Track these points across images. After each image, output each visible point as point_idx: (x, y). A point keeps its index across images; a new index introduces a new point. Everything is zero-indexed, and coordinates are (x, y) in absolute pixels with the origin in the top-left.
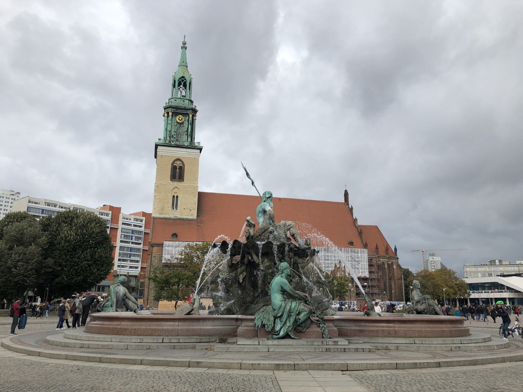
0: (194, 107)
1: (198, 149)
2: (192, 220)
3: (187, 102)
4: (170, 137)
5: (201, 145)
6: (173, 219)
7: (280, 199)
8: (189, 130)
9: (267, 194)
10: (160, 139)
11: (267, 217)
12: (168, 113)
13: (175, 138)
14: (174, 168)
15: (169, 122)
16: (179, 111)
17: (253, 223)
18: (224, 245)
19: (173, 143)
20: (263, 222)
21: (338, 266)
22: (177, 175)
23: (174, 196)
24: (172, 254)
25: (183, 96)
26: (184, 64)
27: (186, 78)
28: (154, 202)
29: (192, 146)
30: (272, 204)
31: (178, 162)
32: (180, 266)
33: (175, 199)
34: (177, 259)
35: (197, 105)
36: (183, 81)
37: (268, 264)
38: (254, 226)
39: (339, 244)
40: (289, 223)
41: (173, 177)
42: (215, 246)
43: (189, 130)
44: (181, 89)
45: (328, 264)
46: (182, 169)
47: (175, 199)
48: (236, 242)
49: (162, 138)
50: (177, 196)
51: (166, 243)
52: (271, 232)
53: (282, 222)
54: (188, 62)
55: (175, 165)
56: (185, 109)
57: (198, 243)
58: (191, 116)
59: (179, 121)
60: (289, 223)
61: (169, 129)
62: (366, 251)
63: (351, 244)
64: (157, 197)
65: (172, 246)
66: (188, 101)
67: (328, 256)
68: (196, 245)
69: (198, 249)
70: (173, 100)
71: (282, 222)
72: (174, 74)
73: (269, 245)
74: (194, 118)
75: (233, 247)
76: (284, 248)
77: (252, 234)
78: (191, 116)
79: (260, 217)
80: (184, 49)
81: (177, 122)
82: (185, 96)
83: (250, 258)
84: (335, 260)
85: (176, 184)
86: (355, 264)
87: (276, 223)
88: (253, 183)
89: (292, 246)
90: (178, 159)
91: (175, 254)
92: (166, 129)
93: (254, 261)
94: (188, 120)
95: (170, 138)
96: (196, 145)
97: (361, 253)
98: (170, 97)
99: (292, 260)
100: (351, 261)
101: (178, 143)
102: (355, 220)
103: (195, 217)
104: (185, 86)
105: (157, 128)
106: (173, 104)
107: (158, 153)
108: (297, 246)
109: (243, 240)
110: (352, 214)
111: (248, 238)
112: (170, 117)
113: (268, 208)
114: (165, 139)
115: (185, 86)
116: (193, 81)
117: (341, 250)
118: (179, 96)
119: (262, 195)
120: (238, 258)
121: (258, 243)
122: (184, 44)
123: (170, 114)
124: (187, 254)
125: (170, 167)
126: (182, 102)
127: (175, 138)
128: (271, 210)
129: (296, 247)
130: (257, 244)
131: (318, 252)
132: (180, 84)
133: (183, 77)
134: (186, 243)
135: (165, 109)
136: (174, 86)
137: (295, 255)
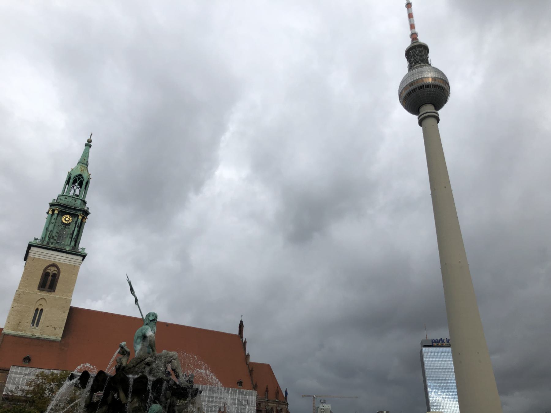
0: (86, 208)
3: (79, 202)
4: (49, 238)
5: (86, 252)
6: (30, 338)
7: (167, 325)
8: (75, 233)
9: (151, 316)
10: (36, 239)
11: (146, 344)
12: (53, 211)
13: (55, 240)
14: (46, 275)
15: (53, 221)
16: (67, 210)
17: (128, 350)
18: (85, 375)
19: (51, 246)
20: (141, 350)
21: (222, 410)
23: (37, 309)
24: (18, 383)
25: (76, 195)
26: (85, 162)
28: (10, 314)
30: (155, 329)
31: (53, 269)
32: (26, 401)
33: (39, 312)
34: (22, 390)
36: (79, 179)
37: (137, 405)
38: (129, 354)
39: (227, 385)
40: (172, 353)
42: (72, 377)
43: (75, 233)
44: (75, 187)
45: (212, 407)
46: (55, 277)
47: (39, 312)
48: (101, 373)
49: (39, 237)
50: (42, 310)
51: (13, 369)
52: (148, 364)
53: (164, 352)
54: (89, 160)
56: (75, 209)
57: (55, 372)
58: (80, 217)
59: (64, 221)
60: (172, 353)
61: (50, 229)
62: (255, 393)
63: (240, 383)
64: (15, 308)
65: (20, 374)
66: (80, 201)
67: (213, 397)
68: (52, 374)
69: (53, 380)
70: (63, 198)
71: (164, 352)
72: (70, 170)
73: (142, 380)
74: (84, 221)
75: (96, 379)
76: (161, 386)
77: (124, 364)
78: (80, 217)
79: (138, 344)
80: (88, 147)
81: (62, 222)
82: (78, 196)
83: (116, 396)
84: (220, 403)
85: (43, 294)
86: (241, 409)
87: (156, 352)
88: (136, 301)
89: (171, 382)
90: (54, 265)
91: (22, 384)
92: (47, 229)
93: (120, 400)
94: (76, 222)
95: (49, 239)
96: (80, 250)
97: (249, 395)
98: (60, 193)
99: (169, 401)
100: (238, 404)
101: (57, 246)
102: (248, 356)
103: (59, 338)
105: (37, 225)
106: (62, 202)
107: (30, 255)
108: (178, 383)
109: (110, 371)
110: (245, 349)
111: (118, 370)
112: (55, 216)
113: (150, 333)
114: (43, 239)
115: (81, 184)
116: (91, 180)
117: (228, 392)
118: (71, 194)
119: (144, 317)
120: (101, 393)
121: (130, 376)
122: (90, 141)
123: (56, 212)
124: (38, 386)
125: (41, 272)
126: (73, 201)
127: (55, 240)
128: (153, 335)
129: (175, 383)
130: (128, 379)
131: (201, 392)
132: (75, 182)
133: (80, 175)
134: (38, 371)
135: (51, 205)
136: (68, 182)
137: (173, 395)
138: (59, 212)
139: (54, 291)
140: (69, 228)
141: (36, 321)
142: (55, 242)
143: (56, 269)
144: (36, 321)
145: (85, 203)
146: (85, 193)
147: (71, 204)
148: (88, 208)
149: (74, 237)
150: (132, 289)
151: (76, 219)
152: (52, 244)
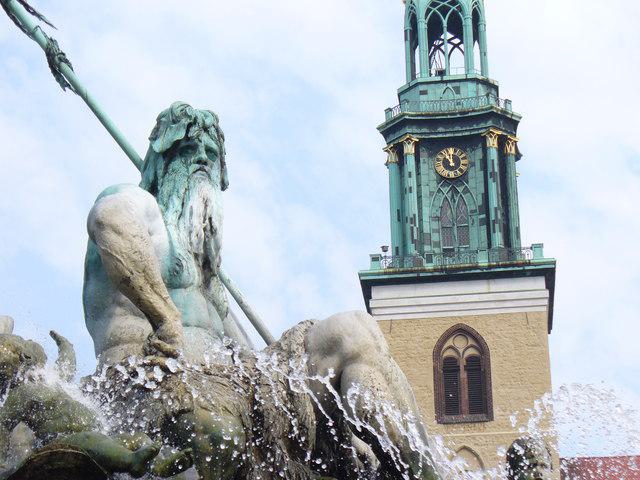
1: (536, 273)
5: (547, 254)
8: (494, 201)
10: (375, 259)
14: (447, 370)
16: (441, 133)
19: (429, 266)
29: (510, 267)
35: (514, 96)
43: (494, 201)
46: (479, 367)
56: (466, 119)
58: (492, 143)
59: (446, 173)
66: (472, 86)
78: (492, 143)
85: (462, 434)
90: (462, 331)
96: (529, 256)
101: (449, 263)
104: (456, 28)
112: (411, 162)
114: (401, 252)
123: (409, 149)
125: (430, 362)
138: (417, 145)
139: (492, 419)
140: (466, 191)
143: (471, 342)
145: (491, 87)
146: (483, 54)
147: (445, 108)
148: (507, 102)
150: (56, 62)
152: (429, 260)
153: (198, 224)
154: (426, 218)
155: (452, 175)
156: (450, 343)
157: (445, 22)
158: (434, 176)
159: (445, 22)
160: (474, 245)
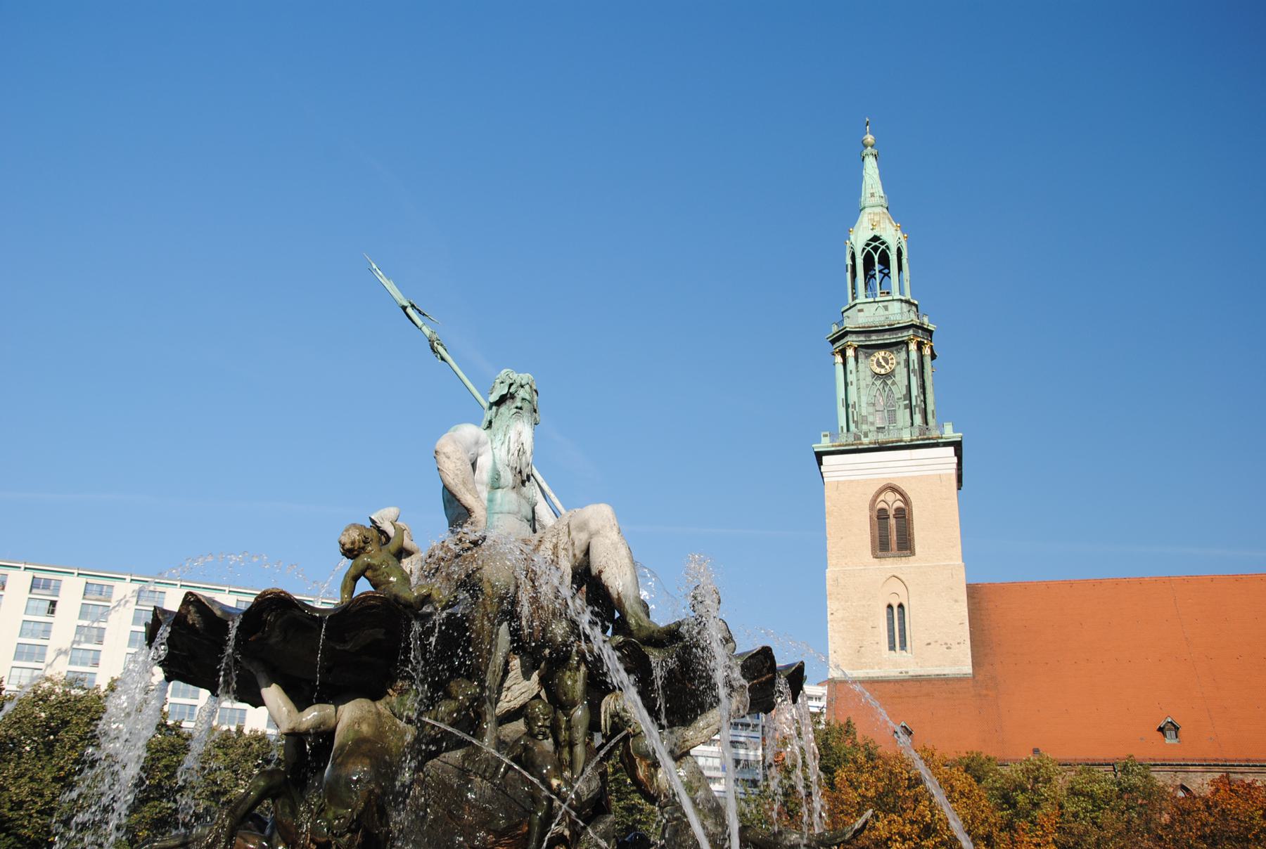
2: (959, 679)
8: (915, 392)
16: (875, 339)
19: (865, 441)
22: (894, 537)
23: (890, 606)
27: (884, 238)
33: (896, 613)
41: (881, 546)
46: (903, 515)
47: (896, 613)
55: (883, 505)
58: (913, 347)
59: (878, 370)
66: (897, 304)
81: (877, 376)
85: (892, 565)
94: (907, 361)
101: (882, 438)
104: (885, 260)
125: (867, 513)
126: (881, 311)
133: (875, 238)
139: (913, 553)
140: (894, 383)
141: (898, 638)
142: (873, 428)
143: (898, 497)
144: (898, 638)
149: (914, 403)
151: (903, 355)
152: (866, 435)
153: (514, 448)
154: (864, 405)
155: (883, 372)
156: (882, 497)
157: (876, 258)
158: (869, 373)
159: (876, 258)
160: (900, 424)
